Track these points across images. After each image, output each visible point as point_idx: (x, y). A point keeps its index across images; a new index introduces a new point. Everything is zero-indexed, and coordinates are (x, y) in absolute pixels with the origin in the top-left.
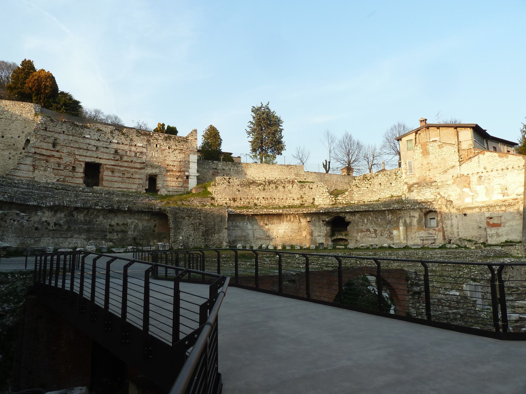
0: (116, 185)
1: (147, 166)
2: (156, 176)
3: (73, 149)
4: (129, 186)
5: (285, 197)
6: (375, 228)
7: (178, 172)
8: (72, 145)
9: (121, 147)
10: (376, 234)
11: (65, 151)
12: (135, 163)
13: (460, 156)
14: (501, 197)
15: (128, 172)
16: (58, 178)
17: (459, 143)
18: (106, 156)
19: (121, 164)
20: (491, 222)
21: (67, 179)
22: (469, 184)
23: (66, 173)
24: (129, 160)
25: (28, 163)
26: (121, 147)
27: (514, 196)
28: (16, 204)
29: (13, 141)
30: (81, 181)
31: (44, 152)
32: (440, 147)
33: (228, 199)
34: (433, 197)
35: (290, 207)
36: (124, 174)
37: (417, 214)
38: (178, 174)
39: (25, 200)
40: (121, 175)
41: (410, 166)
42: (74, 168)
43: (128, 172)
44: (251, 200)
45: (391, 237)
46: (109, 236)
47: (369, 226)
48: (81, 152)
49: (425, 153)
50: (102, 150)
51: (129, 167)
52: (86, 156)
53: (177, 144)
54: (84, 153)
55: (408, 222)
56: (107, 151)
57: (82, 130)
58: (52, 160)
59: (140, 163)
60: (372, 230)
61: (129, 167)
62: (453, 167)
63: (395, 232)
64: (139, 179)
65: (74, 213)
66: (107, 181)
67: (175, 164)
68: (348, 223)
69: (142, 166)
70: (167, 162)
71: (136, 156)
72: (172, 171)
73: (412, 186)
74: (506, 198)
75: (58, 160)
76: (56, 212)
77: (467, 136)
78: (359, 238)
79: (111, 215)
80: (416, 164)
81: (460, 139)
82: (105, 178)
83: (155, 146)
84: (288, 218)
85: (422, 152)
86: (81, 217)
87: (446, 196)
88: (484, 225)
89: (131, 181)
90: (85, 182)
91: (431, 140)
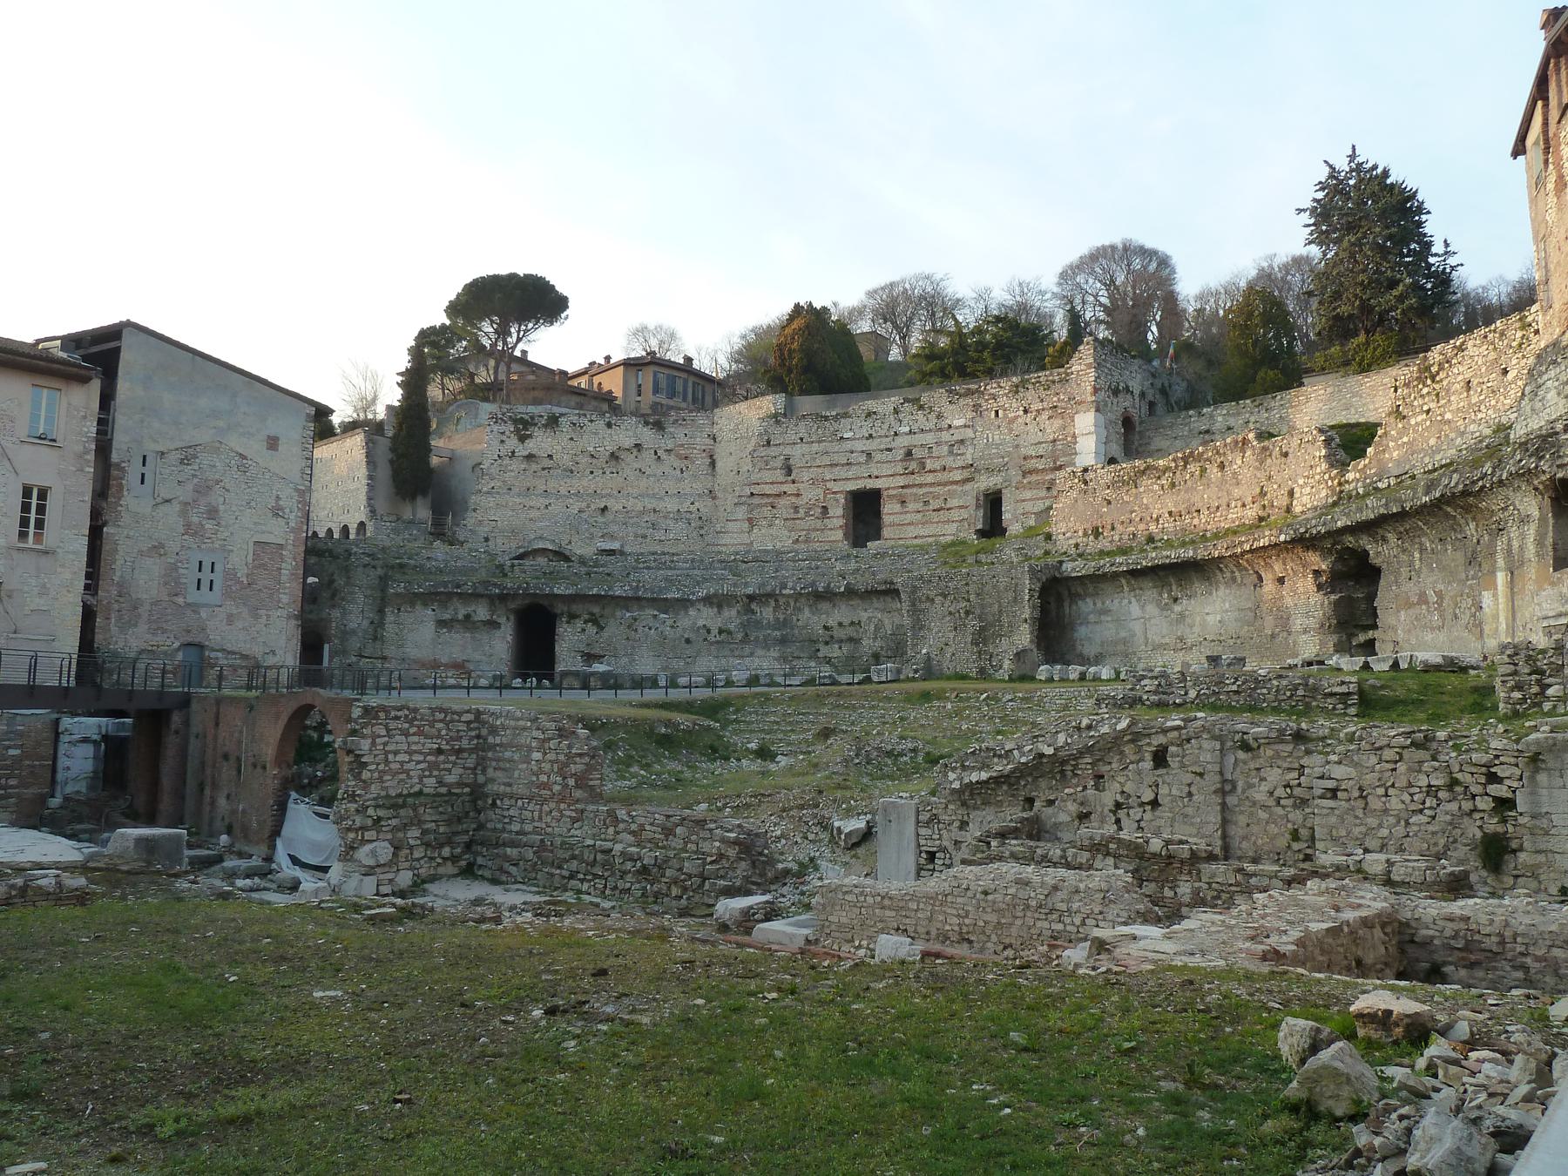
0: (912, 531)
1: (977, 471)
2: (999, 492)
5: (1224, 502)
6: (1440, 587)
8: (818, 463)
9: (919, 439)
15: (935, 497)
16: (794, 536)
19: (918, 479)
21: (813, 535)
23: (811, 522)
24: (937, 465)
25: (740, 516)
26: (919, 439)
28: (647, 600)
30: (839, 535)
31: (768, 490)
36: (926, 503)
39: (661, 590)
40: (919, 506)
44: (1142, 527)
46: (824, 651)
53: (1043, 394)
55: (1515, 544)
57: (836, 426)
58: (783, 502)
63: (1487, 599)
64: (961, 507)
65: (754, 606)
66: (892, 525)
69: (966, 474)
71: (951, 452)
75: (794, 499)
76: (720, 607)
79: (825, 606)
82: (886, 519)
86: (767, 613)
89: (943, 515)
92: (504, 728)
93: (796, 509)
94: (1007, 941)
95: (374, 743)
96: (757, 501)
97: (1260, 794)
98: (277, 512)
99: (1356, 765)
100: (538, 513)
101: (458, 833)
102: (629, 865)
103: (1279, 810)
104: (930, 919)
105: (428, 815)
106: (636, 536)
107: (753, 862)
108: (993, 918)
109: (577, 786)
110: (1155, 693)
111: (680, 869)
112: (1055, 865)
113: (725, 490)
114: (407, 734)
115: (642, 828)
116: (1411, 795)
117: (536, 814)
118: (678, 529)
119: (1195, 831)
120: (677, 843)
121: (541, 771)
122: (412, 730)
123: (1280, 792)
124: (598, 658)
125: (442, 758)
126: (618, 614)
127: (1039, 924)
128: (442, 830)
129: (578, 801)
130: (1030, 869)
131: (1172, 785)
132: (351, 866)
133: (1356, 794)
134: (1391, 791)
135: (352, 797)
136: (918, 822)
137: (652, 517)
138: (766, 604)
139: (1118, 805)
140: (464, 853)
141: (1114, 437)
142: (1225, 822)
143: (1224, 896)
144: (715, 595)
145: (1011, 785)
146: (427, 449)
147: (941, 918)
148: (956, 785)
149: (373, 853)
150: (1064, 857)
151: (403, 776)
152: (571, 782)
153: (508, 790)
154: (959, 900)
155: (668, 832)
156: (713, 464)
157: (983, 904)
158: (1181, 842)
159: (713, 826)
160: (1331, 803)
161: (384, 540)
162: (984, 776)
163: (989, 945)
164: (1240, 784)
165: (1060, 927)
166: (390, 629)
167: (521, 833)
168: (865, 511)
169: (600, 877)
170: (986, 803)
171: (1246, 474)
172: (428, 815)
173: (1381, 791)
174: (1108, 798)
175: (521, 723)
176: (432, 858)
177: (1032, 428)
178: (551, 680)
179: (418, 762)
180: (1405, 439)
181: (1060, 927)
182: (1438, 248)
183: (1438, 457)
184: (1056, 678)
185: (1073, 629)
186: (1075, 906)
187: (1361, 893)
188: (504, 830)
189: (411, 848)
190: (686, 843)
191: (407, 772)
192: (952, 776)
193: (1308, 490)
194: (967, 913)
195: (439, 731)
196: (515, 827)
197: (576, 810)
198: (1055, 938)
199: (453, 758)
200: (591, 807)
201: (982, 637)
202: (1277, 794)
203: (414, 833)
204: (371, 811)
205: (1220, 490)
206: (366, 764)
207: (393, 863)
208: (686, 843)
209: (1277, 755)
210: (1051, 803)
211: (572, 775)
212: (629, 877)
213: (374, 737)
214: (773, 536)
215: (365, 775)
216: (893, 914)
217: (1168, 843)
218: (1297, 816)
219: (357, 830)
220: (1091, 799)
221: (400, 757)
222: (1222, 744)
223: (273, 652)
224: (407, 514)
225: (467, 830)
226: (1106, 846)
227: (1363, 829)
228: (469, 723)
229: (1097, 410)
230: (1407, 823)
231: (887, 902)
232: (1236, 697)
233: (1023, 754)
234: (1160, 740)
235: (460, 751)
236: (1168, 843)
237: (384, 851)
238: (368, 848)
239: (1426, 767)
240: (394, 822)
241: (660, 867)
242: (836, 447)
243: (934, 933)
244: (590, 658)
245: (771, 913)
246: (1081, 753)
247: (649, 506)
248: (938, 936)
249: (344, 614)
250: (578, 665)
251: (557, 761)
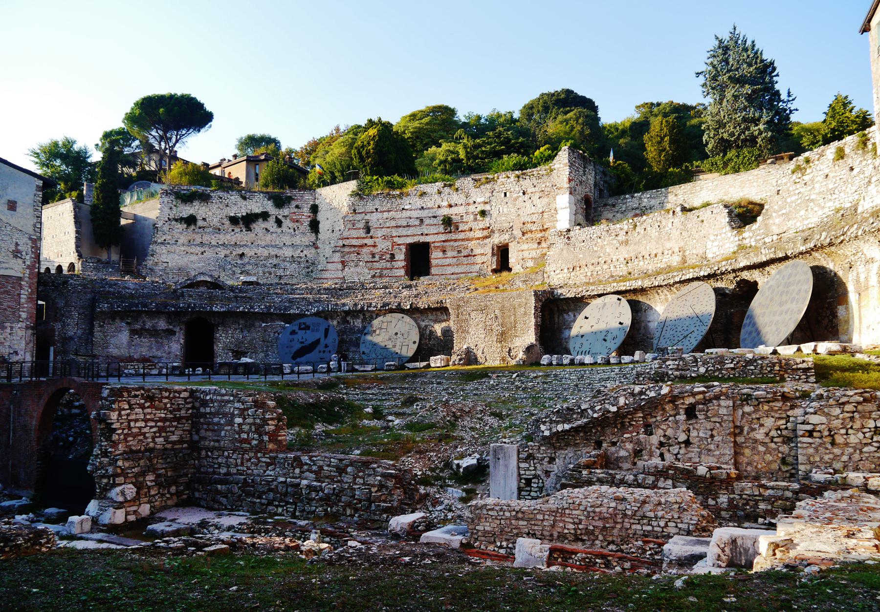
1: (493, 231)
3: (389, 230)
5: (660, 252)
7: (541, 231)
8: (388, 225)
11: (379, 235)
16: (372, 272)
18: (433, 230)
21: (385, 272)
23: (383, 264)
24: (466, 227)
25: (336, 260)
26: (454, 210)
30: (402, 272)
33: (566, 270)
35: (658, 273)
36: (459, 252)
38: (540, 235)
39: (286, 308)
40: (455, 254)
42: (393, 256)
52: (408, 236)
53: (535, 182)
54: (404, 232)
55: (862, 277)
56: (435, 222)
57: (399, 201)
58: (365, 250)
59: (483, 229)
65: (348, 318)
69: (486, 233)
70: (523, 219)
71: (475, 219)
72: (531, 231)
75: (372, 249)
82: (434, 262)
83: (503, 195)
84: (663, 297)
90: (407, 273)
92: (212, 400)
93: (374, 257)
94: (610, 539)
95: (120, 415)
96: (347, 251)
97: (760, 435)
98: (16, 254)
99: (827, 415)
100: (196, 258)
101: (181, 476)
102: (313, 495)
103: (773, 445)
104: (553, 526)
105: (159, 463)
106: (264, 273)
107: (405, 490)
108: (600, 524)
109: (270, 441)
110: (677, 370)
111: (353, 496)
112: (630, 486)
113: (324, 243)
114: (142, 407)
115: (321, 468)
116: (864, 433)
117: (239, 461)
118: (292, 268)
119: (716, 460)
120: (348, 479)
121: (241, 431)
122: (147, 405)
123: (773, 433)
124: (244, 354)
125: (168, 423)
126: (257, 324)
127: (634, 527)
128: (169, 474)
129: (271, 451)
130: (621, 489)
131: (700, 431)
132: (105, 503)
133: (826, 433)
134: (850, 431)
135: (105, 454)
136: (519, 458)
137: (275, 261)
138: (357, 317)
139: (661, 444)
140: (184, 490)
141: (580, 211)
142: (737, 454)
143: (751, 503)
144: (323, 311)
145: (585, 433)
146: (119, 214)
147: (561, 525)
148: (547, 433)
149: (123, 493)
150: (636, 480)
151: (141, 437)
152: (266, 438)
153: (217, 444)
154: (574, 512)
155: (341, 471)
157: (592, 514)
158: (719, 468)
159: (375, 466)
160: (810, 440)
161: (93, 275)
162: (567, 427)
163: (597, 542)
164: (746, 429)
165: (649, 528)
166: (98, 335)
167: (228, 474)
169: (291, 504)
170: (568, 445)
171: (675, 233)
172: (159, 463)
173: (843, 431)
174: (655, 439)
175: (226, 398)
176: (163, 495)
177: (528, 203)
178: (212, 368)
179: (151, 427)
180: (784, 211)
181: (649, 528)
182: (784, 96)
183: (806, 222)
184: (554, 363)
185: (561, 332)
186: (660, 514)
187: (866, 500)
188: (214, 473)
189: (149, 488)
190: (355, 478)
191: (144, 434)
192: (543, 427)
193: (716, 244)
194: (581, 521)
195: (165, 404)
196: (223, 470)
197: (270, 458)
198: (646, 536)
199: (175, 424)
200: (281, 456)
201: (503, 337)
202: (771, 434)
203: (150, 477)
204: (120, 463)
205: (657, 243)
206: (115, 430)
207: (136, 500)
208: (355, 478)
209: (771, 409)
210: (614, 444)
211: (266, 434)
212: (314, 503)
213: (120, 410)
215: (115, 437)
216: (525, 523)
217: (710, 468)
218: (785, 449)
219: (109, 477)
220: (643, 440)
221: (139, 424)
222: (734, 403)
223: (16, 353)
224: (104, 257)
225: (189, 473)
226: (667, 472)
227: (831, 456)
228: (185, 399)
229: (571, 193)
230: (861, 452)
231: (520, 515)
232: (733, 372)
233: (595, 412)
234: (691, 400)
235: (181, 418)
236: (710, 468)
237: (130, 490)
238: (118, 489)
239: (874, 415)
240: (135, 470)
241: (337, 495)
242: (399, 215)
243: (556, 534)
244: (238, 354)
245: (430, 526)
246: (636, 410)
247: (273, 253)
248: (559, 537)
249: (63, 326)
250: (230, 359)
251: (254, 424)
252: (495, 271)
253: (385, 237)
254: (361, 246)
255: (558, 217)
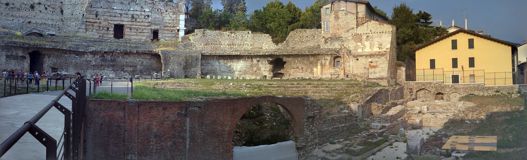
0: (133, 37)
2: (158, 30)
4: (141, 38)
10: (303, 71)
12: (145, 22)
13: (357, 22)
14: (378, 50)
17: (357, 13)
18: (126, 19)
20: (372, 64)
22: (361, 40)
23: (104, 32)
24: (141, 21)
27: (385, 50)
29: (77, 16)
30: (112, 36)
31: (91, 20)
32: (346, 14)
34: (339, 47)
36: (137, 30)
37: (329, 58)
41: (327, 26)
43: (140, 29)
45: (312, 72)
47: (299, 65)
48: (112, 18)
49: (337, 18)
50: (124, 15)
51: (141, 26)
54: (114, 19)
55: (323, 63)
58: (96, 25)
60: (300, 68)
61: (141, 26)
62: (353, 28)
63: (315, 69)
67: (170, 21)
68: (285, 63)
71: (145, 18)
73: (327, 39)
74: (381, 50)
77: (362, 8)
78: (291, 73)
80: (331, 25)
81: (358, 11)
82: (126, 33)
85: (335, 17)
87: (347, 47)
88: (367, 66)
89: (142, 34)
91: (341, 9)
93: (100, 27)
156: (62, 12)
168: (119, 30)
214: (93, 34)
252: (152, 40)
253: (105, 20)
254: (94, 23)
255: (180, 23)
